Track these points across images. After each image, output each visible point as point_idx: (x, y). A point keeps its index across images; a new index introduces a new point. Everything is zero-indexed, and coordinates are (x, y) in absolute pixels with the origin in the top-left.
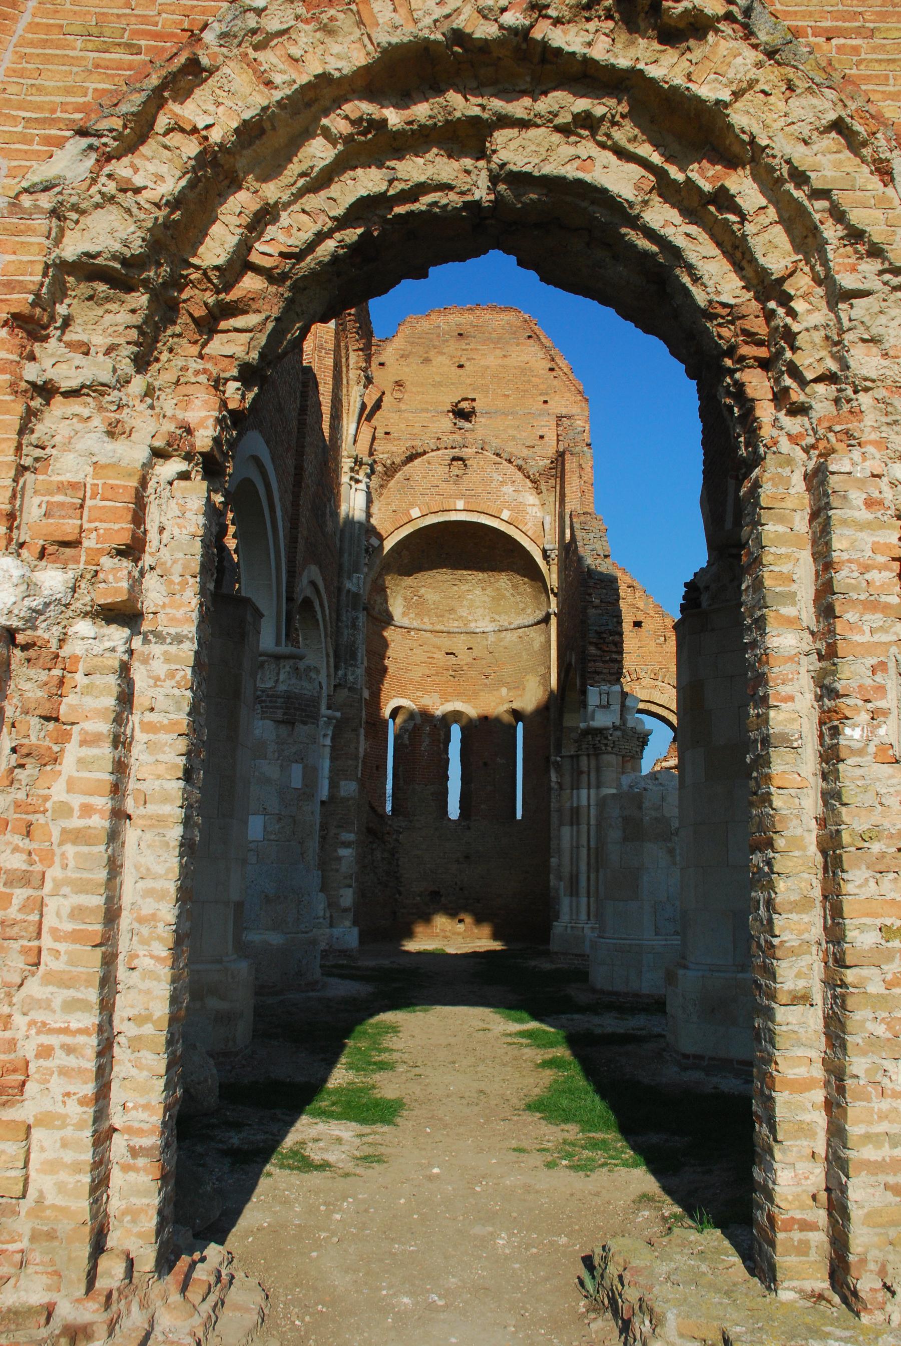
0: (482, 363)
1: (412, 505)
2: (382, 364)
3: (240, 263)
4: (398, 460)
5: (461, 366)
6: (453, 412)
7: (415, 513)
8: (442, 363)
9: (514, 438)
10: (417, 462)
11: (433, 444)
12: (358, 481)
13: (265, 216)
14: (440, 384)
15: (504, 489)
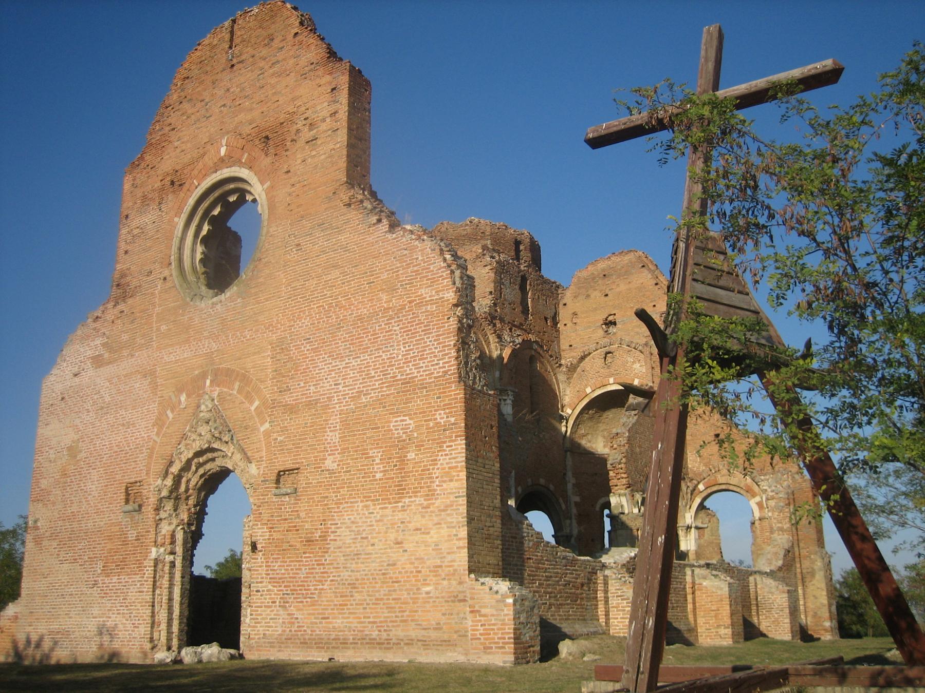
0: (618, 290)
1: (586, 386)
2: (565, 304)
3: (187, 490)
4: (575, 361)
5: (607, 295)
6: (606, 324)
7: (588, 390)
8: (596, 295)
9: (638, 333)
10: (587, 360)
11: (593, 347)
12: (505, 400)
13: (188, 481)
14: (596, 309)
15: (634, 366)
